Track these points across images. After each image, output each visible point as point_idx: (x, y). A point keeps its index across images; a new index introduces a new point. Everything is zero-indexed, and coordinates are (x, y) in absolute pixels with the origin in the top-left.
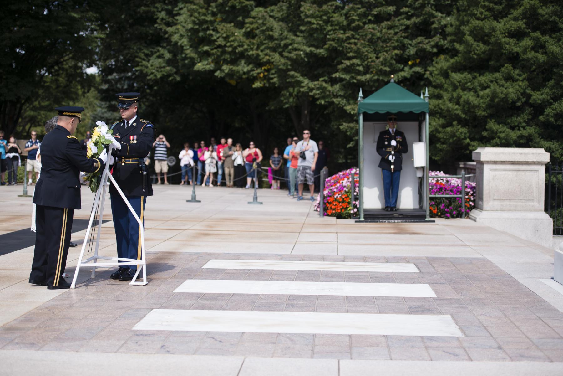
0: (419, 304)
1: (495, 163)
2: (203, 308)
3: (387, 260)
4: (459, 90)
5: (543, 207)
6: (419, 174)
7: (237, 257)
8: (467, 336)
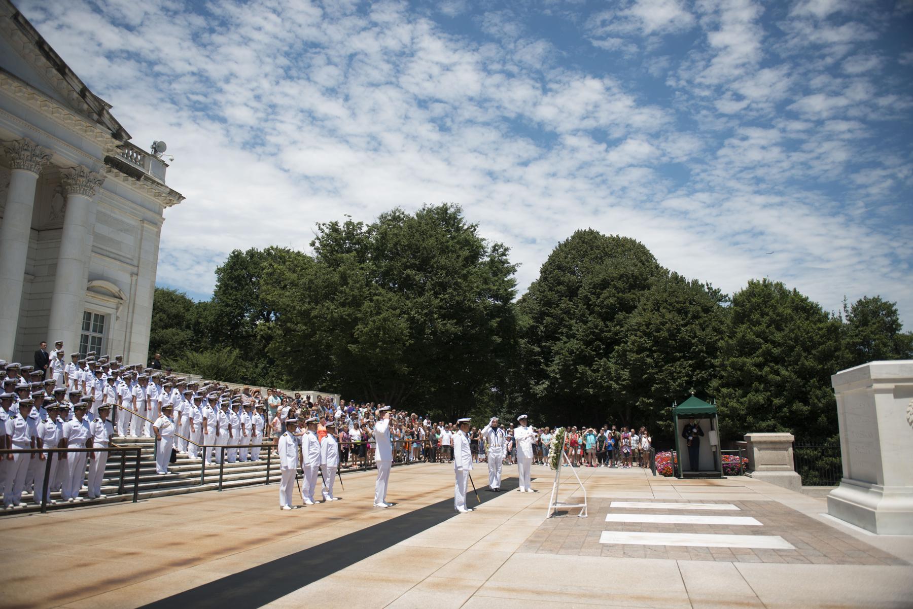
0: (756, 529)
1: (760, 443)
2: (630, 531)
3: (716, 502)
4: (727, 399)
5: (794, 469)
6: (714, 449)
7: (626, 500)
8: (800, 549)
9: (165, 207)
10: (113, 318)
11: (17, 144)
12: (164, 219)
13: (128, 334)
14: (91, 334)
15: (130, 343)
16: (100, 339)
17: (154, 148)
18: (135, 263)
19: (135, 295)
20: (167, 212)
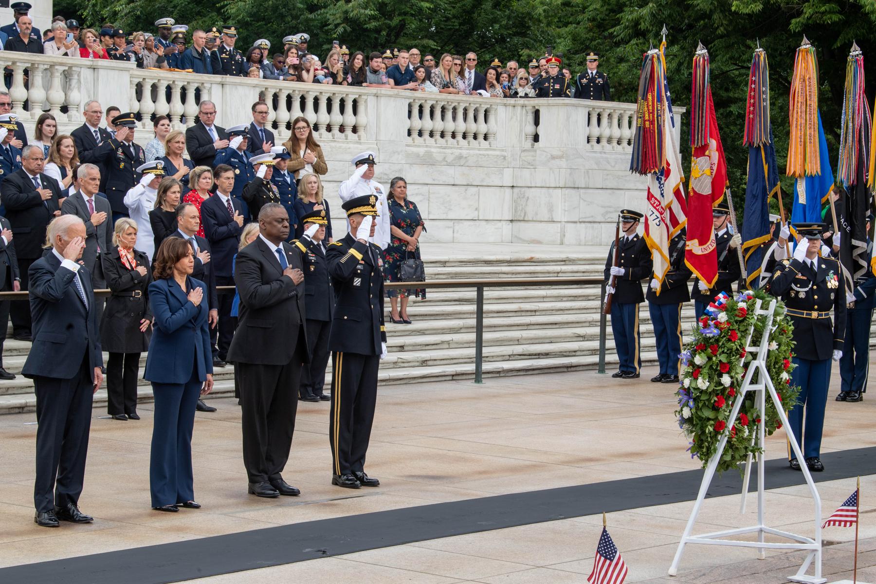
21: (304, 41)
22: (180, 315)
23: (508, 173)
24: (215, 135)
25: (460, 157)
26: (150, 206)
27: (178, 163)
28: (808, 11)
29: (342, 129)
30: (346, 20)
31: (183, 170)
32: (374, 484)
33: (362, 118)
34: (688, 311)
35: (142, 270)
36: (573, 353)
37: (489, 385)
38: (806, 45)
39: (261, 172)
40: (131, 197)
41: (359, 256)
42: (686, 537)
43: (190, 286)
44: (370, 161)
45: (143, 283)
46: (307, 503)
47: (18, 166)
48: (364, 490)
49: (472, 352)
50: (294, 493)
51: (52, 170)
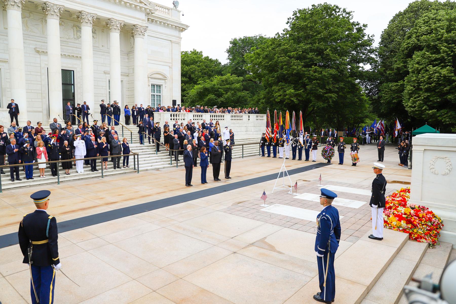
9: (182, 32)
10: (164, 86)
11: (109, 21)
12: (181, 38)
13: (171, 92)
14: (156, 94)
15: (172, 96)
16: (160, 96)
17: (174, 4)
18: (171, 62)
19: (172, 75)
20: (183, 34)
21: (216, 107)
22: (204, 157)
23: (245, 124)
24: (205, 124)
25: (238, 123)
26: (197, 136)
27: (201, 129)
28: (286, 101)
29: (222, 120)
30: (221, 101)
31: (202, 130)
32: (231, 178)
33: (225, 118)
34: (272, 147)
35: (197, 146)
36: (256, 153)
37: (244, 158)
38: (287, 111)
39: (212, 130)
40: (194, 134)
41: (228, 148)
42: (274, 188)
43: (206, 153)
44: (227, 127)
45: (197, 148)
46: (222, 182)
47: (179, 131)
48: (230, 179)
49: (242, 153)
50: (220, 180)
51: (184, 131)
